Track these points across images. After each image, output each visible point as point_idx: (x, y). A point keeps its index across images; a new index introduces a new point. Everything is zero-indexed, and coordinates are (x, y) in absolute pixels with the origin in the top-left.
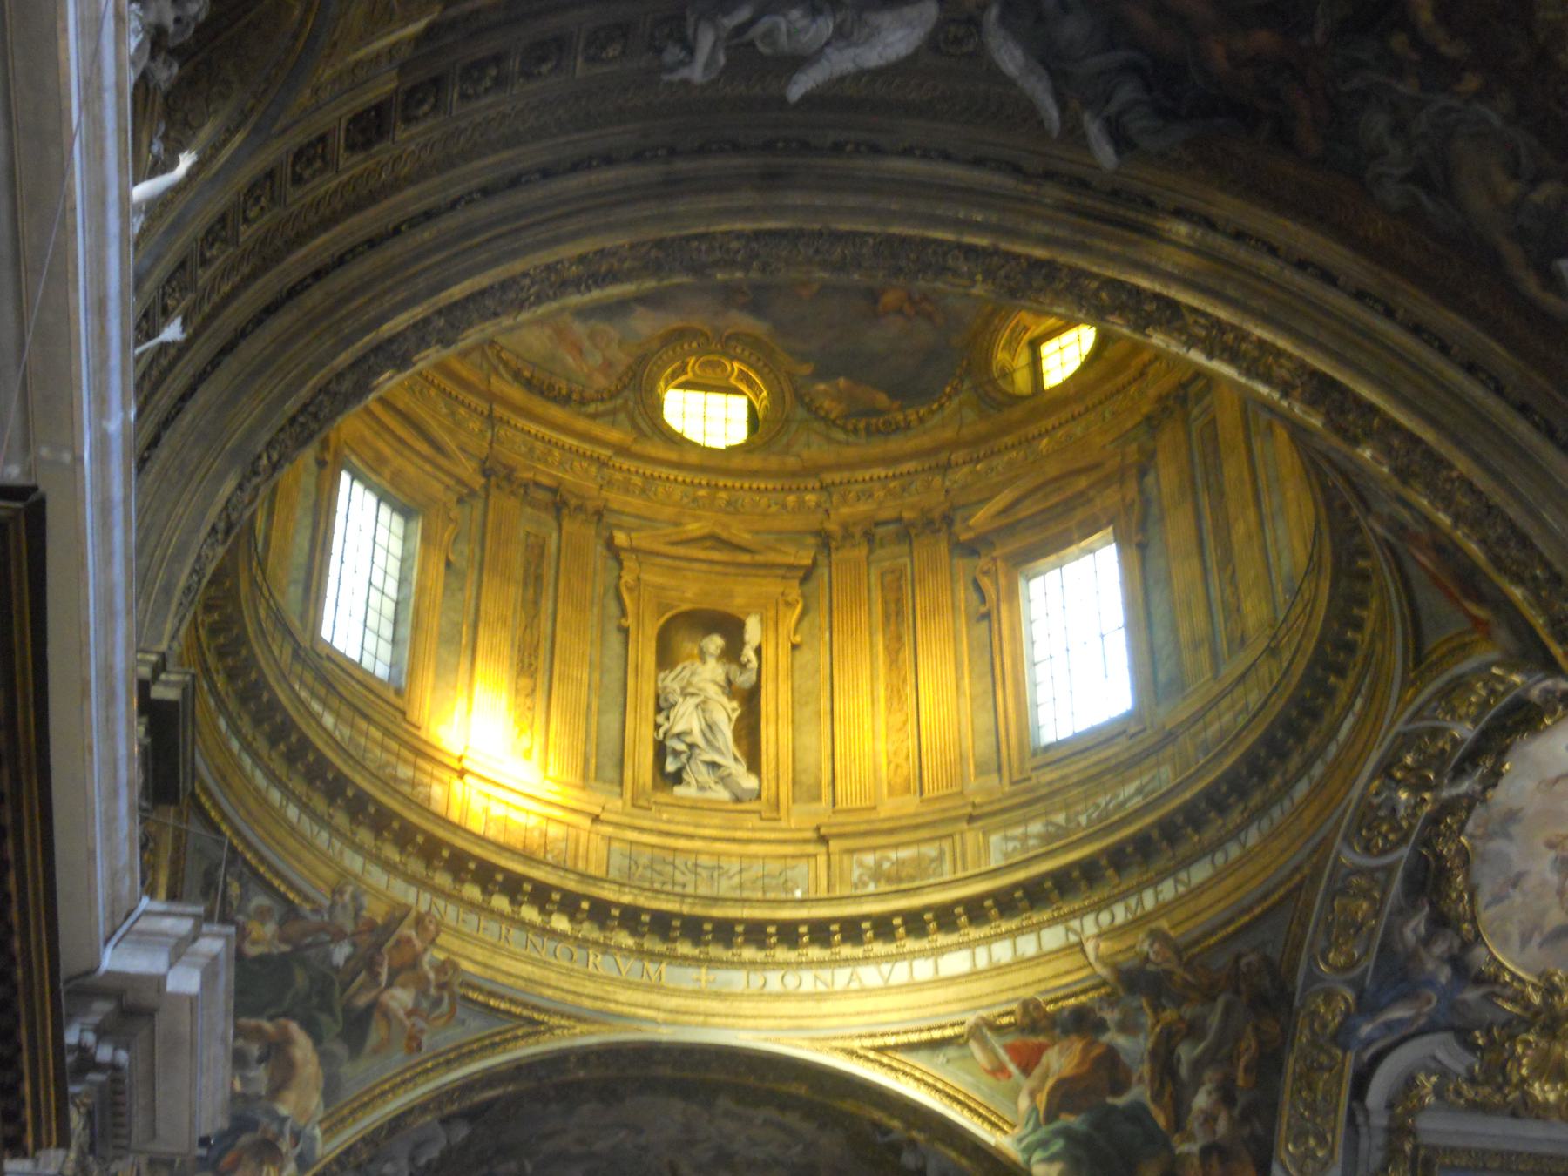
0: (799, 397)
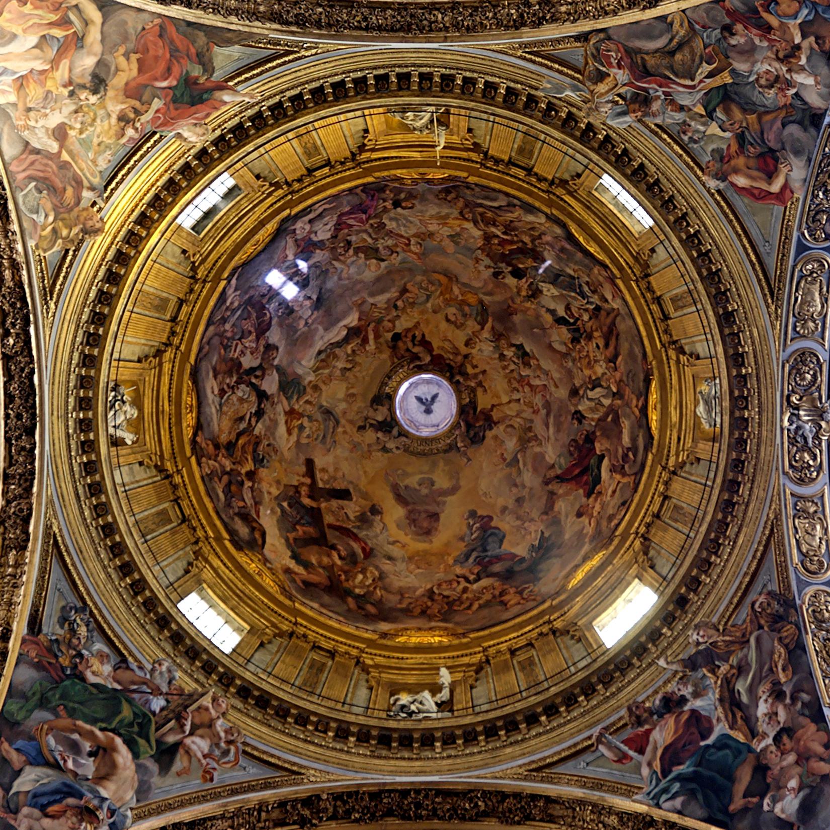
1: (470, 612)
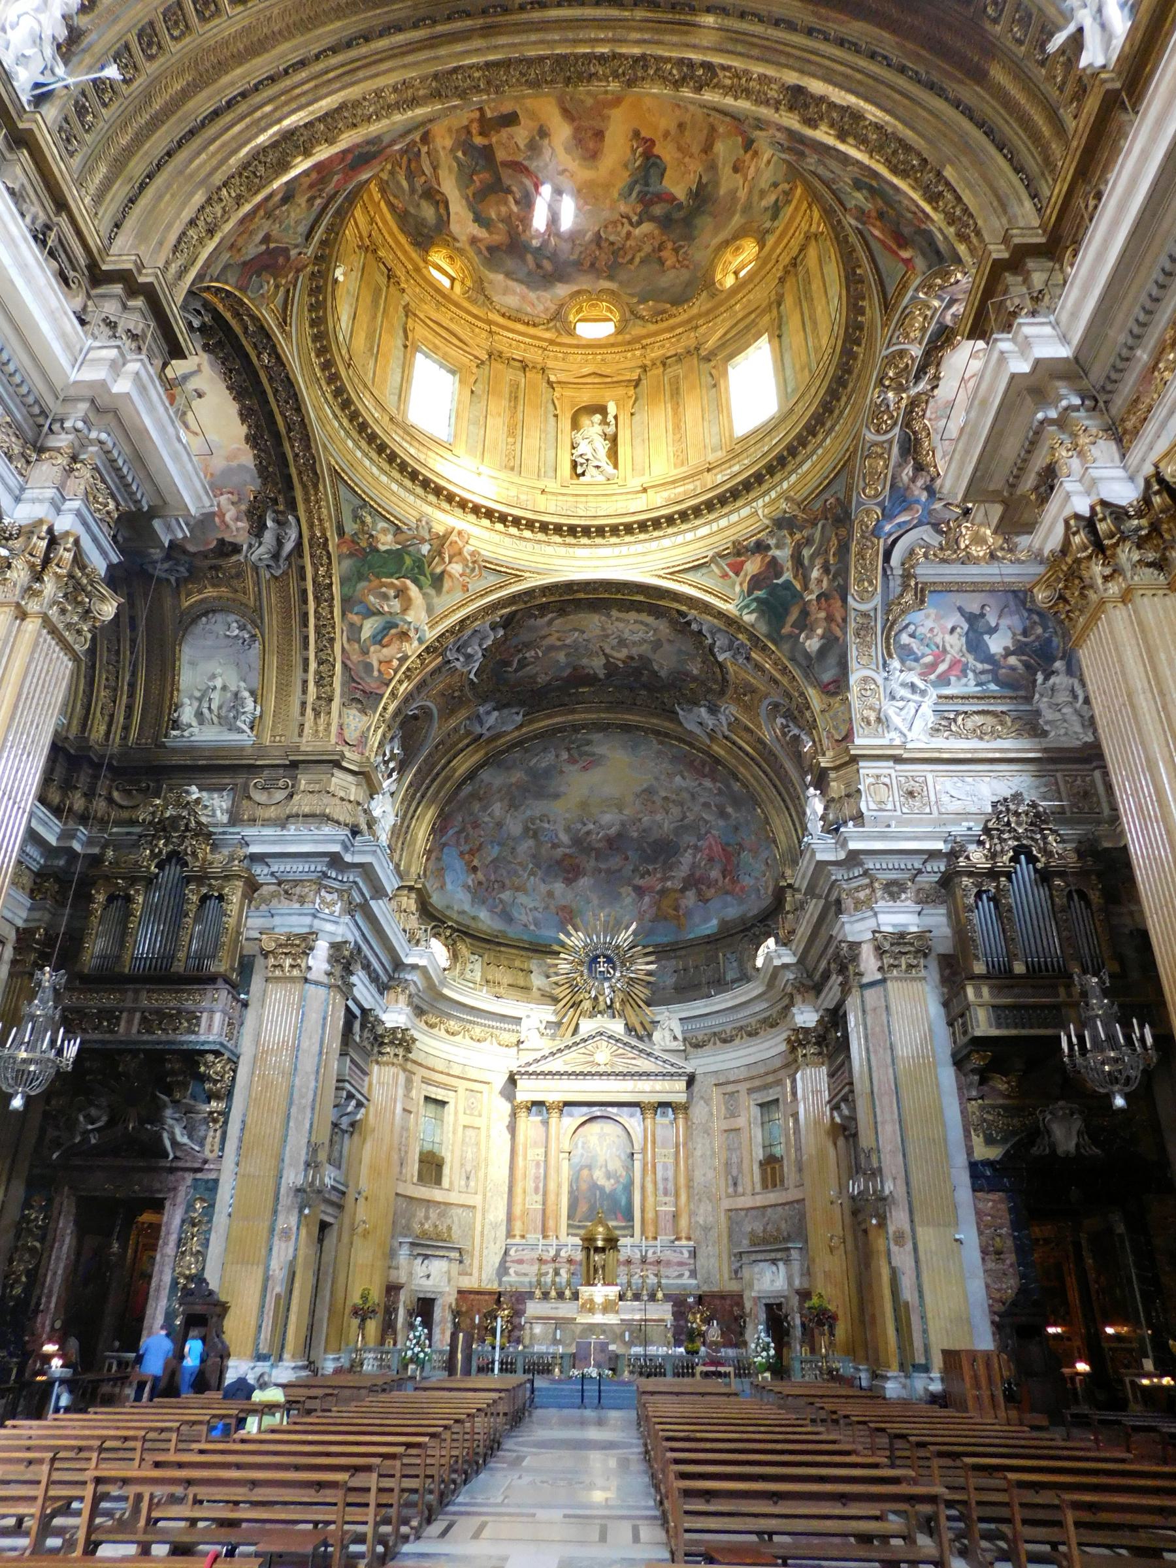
0: (632, 312)
1: (632, 267)
